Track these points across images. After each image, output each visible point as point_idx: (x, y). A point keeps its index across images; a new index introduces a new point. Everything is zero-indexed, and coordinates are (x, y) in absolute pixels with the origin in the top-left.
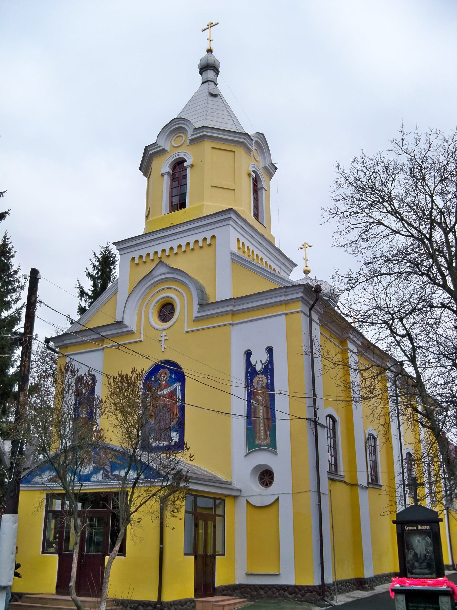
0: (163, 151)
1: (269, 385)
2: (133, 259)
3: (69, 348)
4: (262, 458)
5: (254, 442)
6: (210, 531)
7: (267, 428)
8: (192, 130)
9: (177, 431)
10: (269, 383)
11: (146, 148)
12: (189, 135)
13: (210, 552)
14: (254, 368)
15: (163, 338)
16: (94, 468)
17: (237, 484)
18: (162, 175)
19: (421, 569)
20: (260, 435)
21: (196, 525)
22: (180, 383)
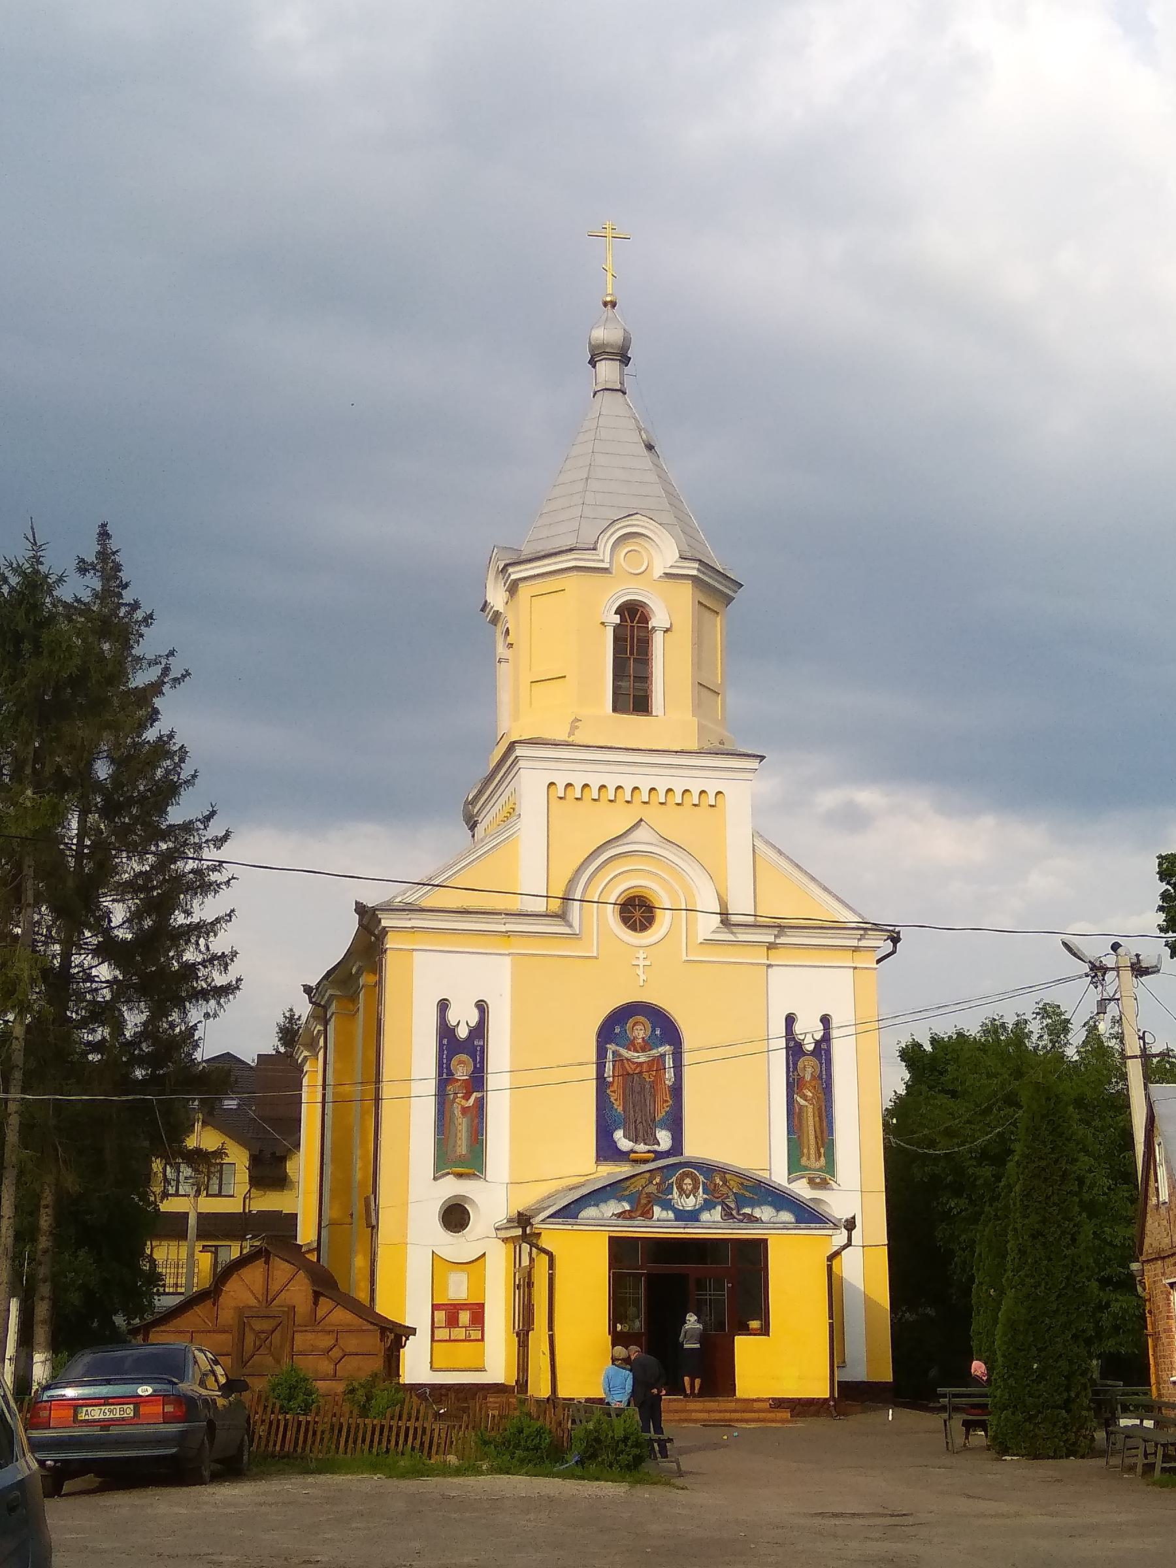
15: (641, 963)
16: (705, 1200)
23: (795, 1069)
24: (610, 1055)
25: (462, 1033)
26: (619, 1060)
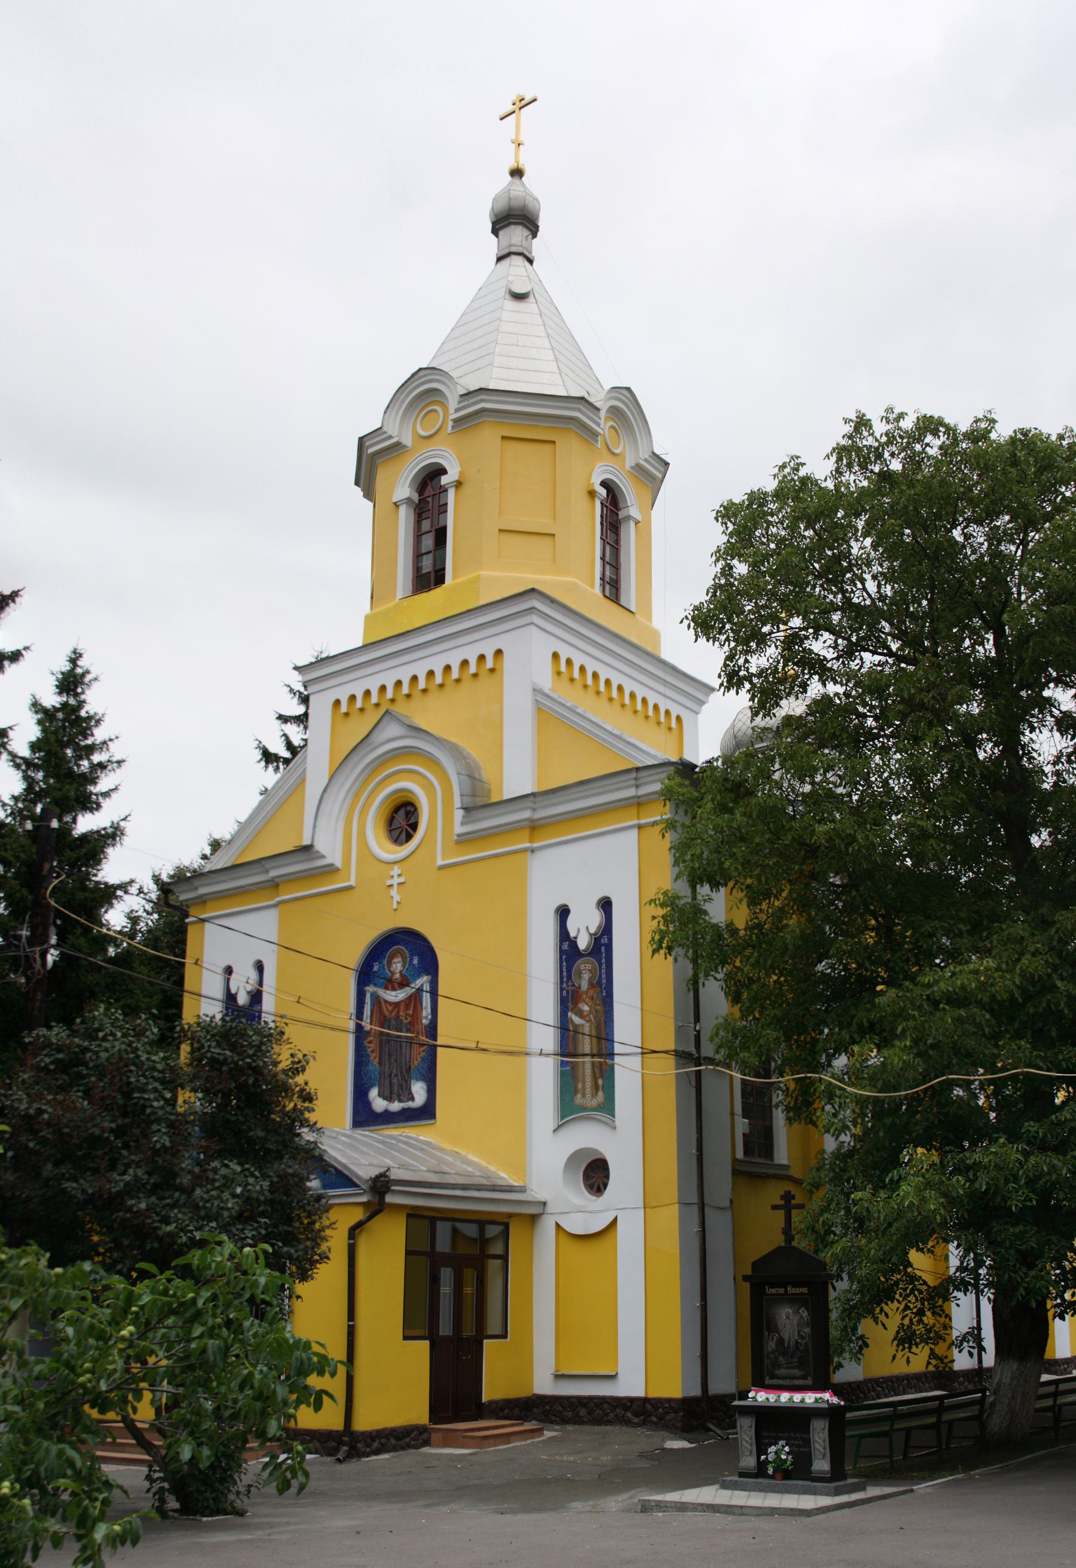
0: (397, 448)
1: (604, 981)
2: (337, 703)
3: (209, 904)
4: (587, 1136)
5: (572, 1100)
6: (469, 1290)
7: (597, 1071)
8: (457, 398)
9: (423, 1079)
10: (604, 976)
11: (361, 440)
12: (452, 410)
13: (468, 1331)
14: (573, 943)
15: (396, 881)
17: (538, 1191)
18: (396, 505)
19: (788, 1368)
20: (584, 1087)
21: (435, 1280)
22: (430, 977)
23: (569, 977)
24: (368, 999)
25: (242, 999)
26: (376, 999)
